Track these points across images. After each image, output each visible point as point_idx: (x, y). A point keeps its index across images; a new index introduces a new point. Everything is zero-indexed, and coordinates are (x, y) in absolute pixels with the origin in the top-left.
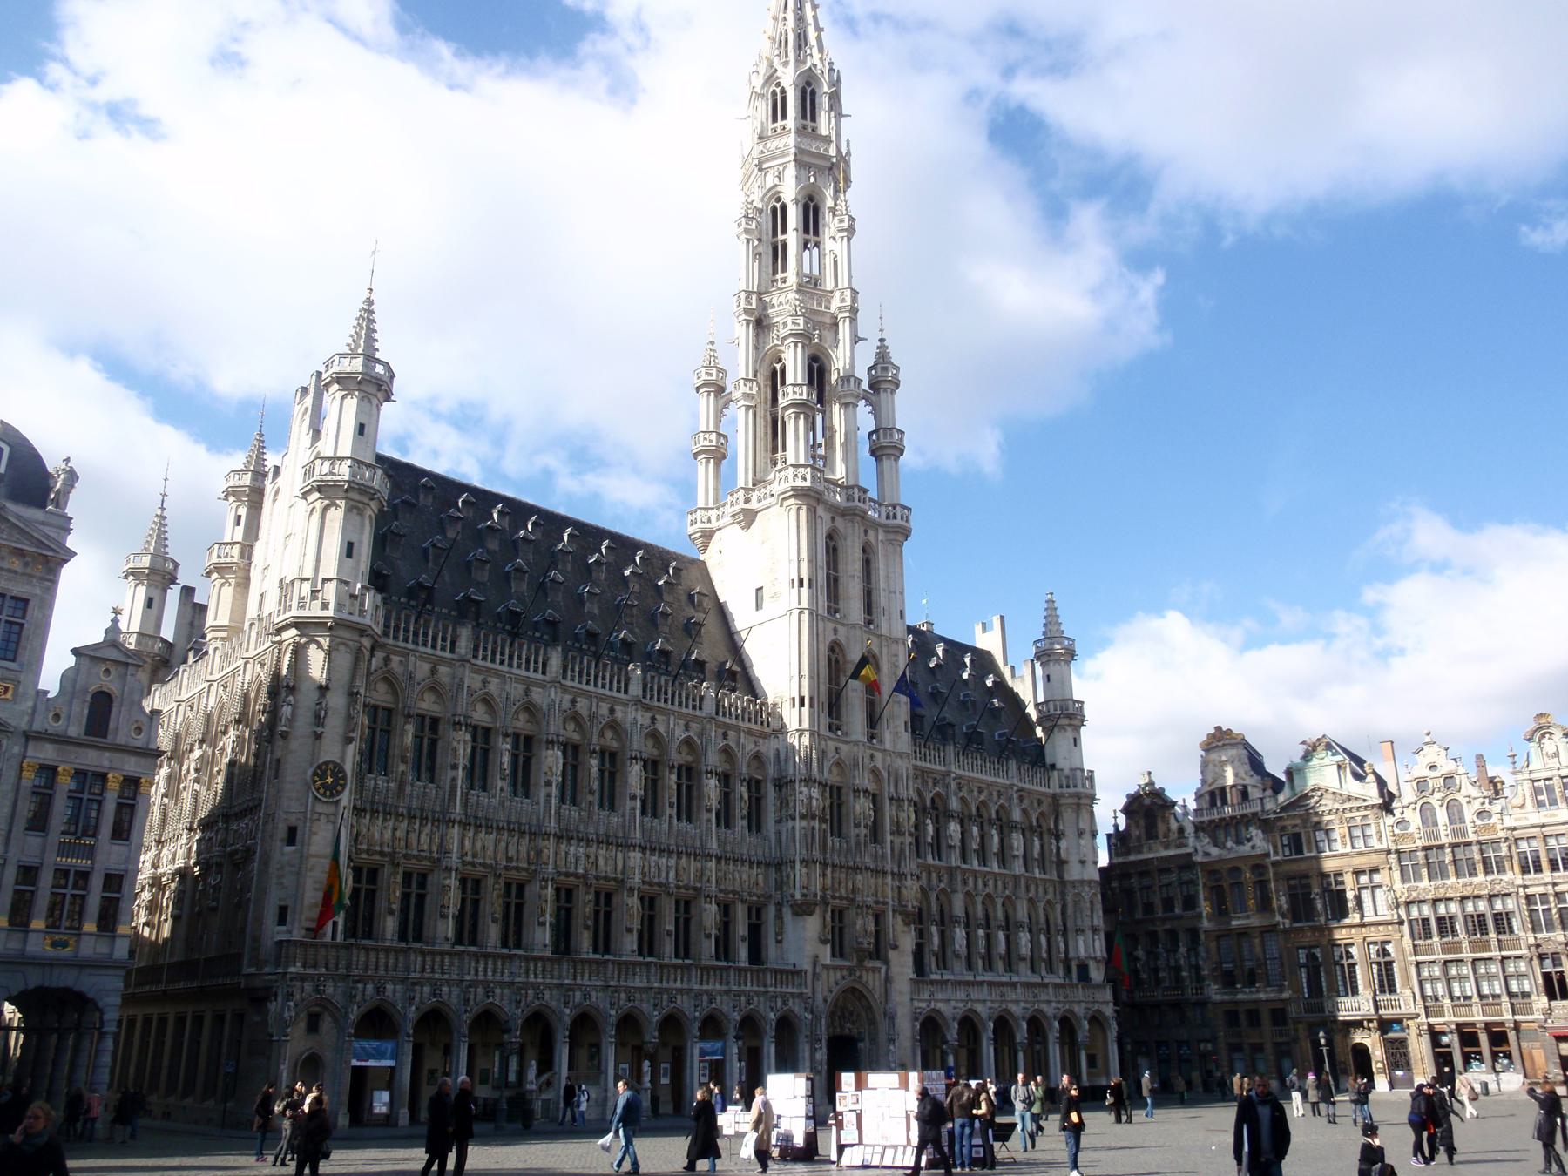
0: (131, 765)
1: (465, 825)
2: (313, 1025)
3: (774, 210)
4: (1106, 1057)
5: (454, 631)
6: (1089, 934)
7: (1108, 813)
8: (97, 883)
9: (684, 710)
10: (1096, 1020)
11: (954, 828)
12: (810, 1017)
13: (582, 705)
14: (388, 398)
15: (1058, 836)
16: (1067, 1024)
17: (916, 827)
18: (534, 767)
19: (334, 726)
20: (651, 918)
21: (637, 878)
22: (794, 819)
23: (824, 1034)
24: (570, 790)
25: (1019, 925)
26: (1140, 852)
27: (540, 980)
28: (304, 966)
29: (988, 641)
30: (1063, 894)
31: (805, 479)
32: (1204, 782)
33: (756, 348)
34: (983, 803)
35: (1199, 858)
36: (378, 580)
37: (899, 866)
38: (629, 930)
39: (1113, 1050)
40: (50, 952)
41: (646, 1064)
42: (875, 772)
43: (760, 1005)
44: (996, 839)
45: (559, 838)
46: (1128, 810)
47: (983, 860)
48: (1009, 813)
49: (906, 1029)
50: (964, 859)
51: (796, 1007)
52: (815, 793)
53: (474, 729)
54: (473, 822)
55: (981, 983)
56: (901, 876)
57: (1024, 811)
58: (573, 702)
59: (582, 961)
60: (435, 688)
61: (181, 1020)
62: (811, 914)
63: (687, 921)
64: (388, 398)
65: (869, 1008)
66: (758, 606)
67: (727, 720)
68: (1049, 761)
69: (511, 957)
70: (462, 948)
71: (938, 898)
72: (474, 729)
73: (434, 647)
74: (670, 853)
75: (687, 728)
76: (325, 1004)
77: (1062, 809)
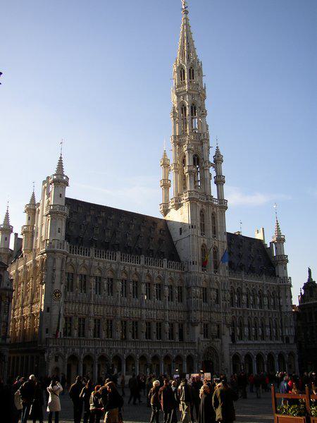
3: (182, 109)
13: (127, 268)
14: (68, 186)
17: (232, 298)
19: (57, 280)
20: (150, 329)
21: (145, 317)
23: (202, 360)
24: (125, 292)
29: (259, 236)
36: (68, 237)
39: (297, 363)
42: (217, 282)
43: (181, 352)
49: (228, 359)
50: (248, 307)
54: (96, 304)
56: (226, 313)
58: (124, 267)
59: (129, 341)
61: (23, 358)
63: (160, 329)
64: (68, 186)
66: (181, 234)
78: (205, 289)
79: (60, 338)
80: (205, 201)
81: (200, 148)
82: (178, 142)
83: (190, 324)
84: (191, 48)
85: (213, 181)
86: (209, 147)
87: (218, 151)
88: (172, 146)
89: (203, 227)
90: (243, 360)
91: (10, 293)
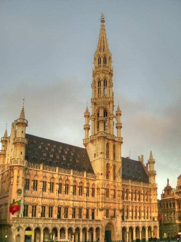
1: (42, 198)
4: (157, 233)
5: (40, 165)
6: (155, 212)
7: (160, 191)
9: (80, 177)
10: (155, 227)
11: (130, 195)
12: (102, 228)
13: (63, 177)
15: (150, 195)
16: (150, 228)
21: (72, 205)
22: (100, 195)
25: (142, 211)
26: (166, 197)
27: (55, 223)
28: (17, 221)
30: (151, 205)
31: (102, 134)
32: (177, 185)
33: (95, 109)
34: (136, 190)
35: (176, 198)
36: (26, 158)
37: (119, 202)
38: (71, 214)
41: (73, 236)
42: (115, 186)
44: (138, 196)
45: (58, 199)
46: (165, 190)
48: (141, 192)
50: (132, 200)
51: (100, 226)
52: (103, 190)
53: (43, 182)
55: (134, 221)
57: (144, 191)
58: (61, 176)
60: (36, 175)
62: (102, 211)
65: (113, 226)
67: (88, 178)
68: (149, 182)
69: (50, 219)
70: (42, 218)
71: (127, 207)
72: (43, 182)
73: (36, 168)
74: (78, 201)
75: (81, 180)
77: (151, 190)
78: (107, 190)
79: (21, 218)
80: (110, 138)
83: (98, 210)
85: (115, 126)
86: (113, 106)
88: (90, 105)
90: (128, 230)
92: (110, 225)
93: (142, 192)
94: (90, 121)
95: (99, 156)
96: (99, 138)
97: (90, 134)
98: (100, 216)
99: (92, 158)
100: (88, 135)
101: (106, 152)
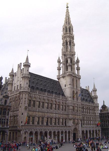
0: (9, 107)
1: (38, 112)
2: (25, 134)
3: (66, 42)
8: (6, 120)
10: (99, 130)
11: (85, 110)
13: (49, 98)
16: (96, 131)
18: (44, 105)
19: (26, 102)
25: (91, 120)
26: (103, 112)
34: (87, 107)
40: (2, 127)
42: (77, 104)
47: (88, 114)
49: (81, 132)
56: (80, 116)
58: (48, 98)
59: (49, 126)
60: (35, 97)
66: (65, 87)
68: (94, 102)
76: (26, 131)
81: (72, 57)
82: (64, 55)
83: (69, 120)
84: (69, 20)
87: (78, 58)
88: (61, 55)
89: (73, 84)
91: (10, 107)
92: (75, 129)
93: (91, 109)
94: (61, 65)
95: (68, 86)
96: (68, 75)
97: (61, 73)
98: (70, 123)
99: (63, 87)
100: (60, 73)
101: (72, 84)
